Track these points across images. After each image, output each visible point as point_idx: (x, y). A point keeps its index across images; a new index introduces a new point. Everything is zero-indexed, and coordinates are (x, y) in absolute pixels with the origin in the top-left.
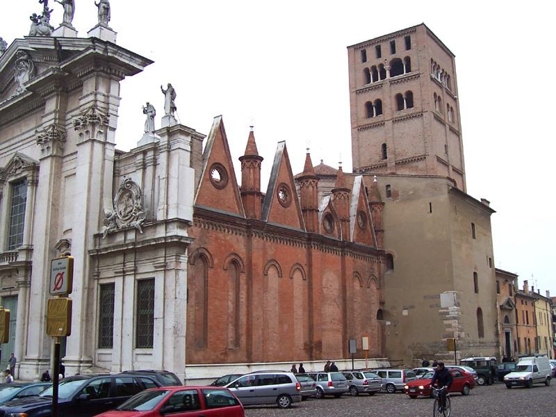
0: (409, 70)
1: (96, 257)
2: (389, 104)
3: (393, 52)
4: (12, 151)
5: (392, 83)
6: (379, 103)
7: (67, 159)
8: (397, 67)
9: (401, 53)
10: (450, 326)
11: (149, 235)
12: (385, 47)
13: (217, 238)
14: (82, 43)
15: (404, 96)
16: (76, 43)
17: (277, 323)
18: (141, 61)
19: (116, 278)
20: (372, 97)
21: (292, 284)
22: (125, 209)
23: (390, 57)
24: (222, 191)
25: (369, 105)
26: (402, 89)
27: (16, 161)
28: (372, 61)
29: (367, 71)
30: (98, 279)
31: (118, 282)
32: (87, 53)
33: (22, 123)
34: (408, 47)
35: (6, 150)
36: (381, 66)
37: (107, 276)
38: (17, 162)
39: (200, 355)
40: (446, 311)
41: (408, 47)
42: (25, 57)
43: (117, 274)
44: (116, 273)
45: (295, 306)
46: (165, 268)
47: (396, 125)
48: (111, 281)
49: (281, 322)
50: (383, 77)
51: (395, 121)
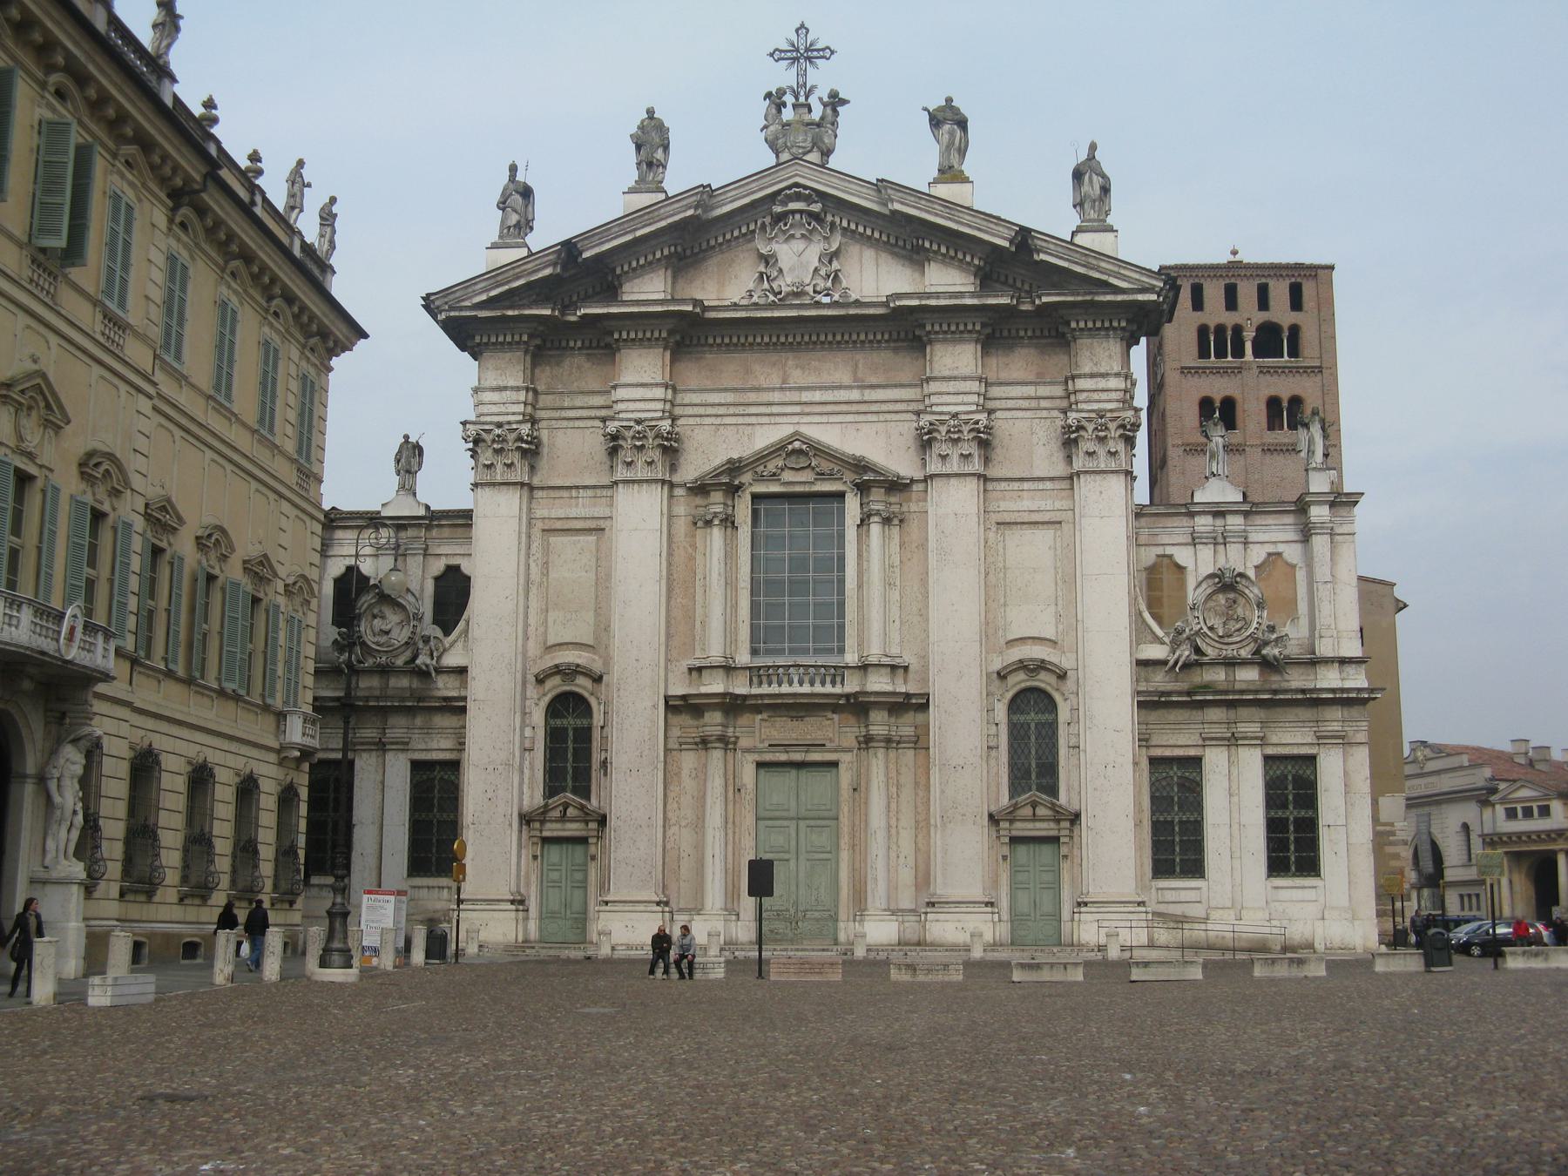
0: (1294, 352)
1: (1148, 704)
2: (1253, 414)
3: (1263, 304)
4: (765, 420)
5: (1264, 371)
6: (1229, 406)
7: (1003, 485)
8: (1270, 340)
9: (1281, 315)
10: (1396, 856)
11: (1296, 680)
12: (1247, 293)
14: (1122, 271)
15: (1285, 404)
16: (1103, 265)
19: (1208, 750)
20: (1218, 388)
22: (1224, 623)
23: (1260, 317)
25: (1206, 405)
26: (1285, 388)
27: (794, 451)
28: (1215, 313)
29: (1203, 331)
30: (1148, 747)
31: (1215, 761)
32: (1140, 297)
33: (790, 360)
34: (1296, 303)
35: (722, 410)
36: (1238, 330)
37: (1178, 739)
38: (799, 451)
40: (1388, 828)
41: (1296, 303)
42: (816, 207)
43: (1207, 741)
44: (1204, 739)
46: (1344, 741)
47: (1268, 458)
48: (1192, 752)
50: (1239, 352)
51: (1269, 450)
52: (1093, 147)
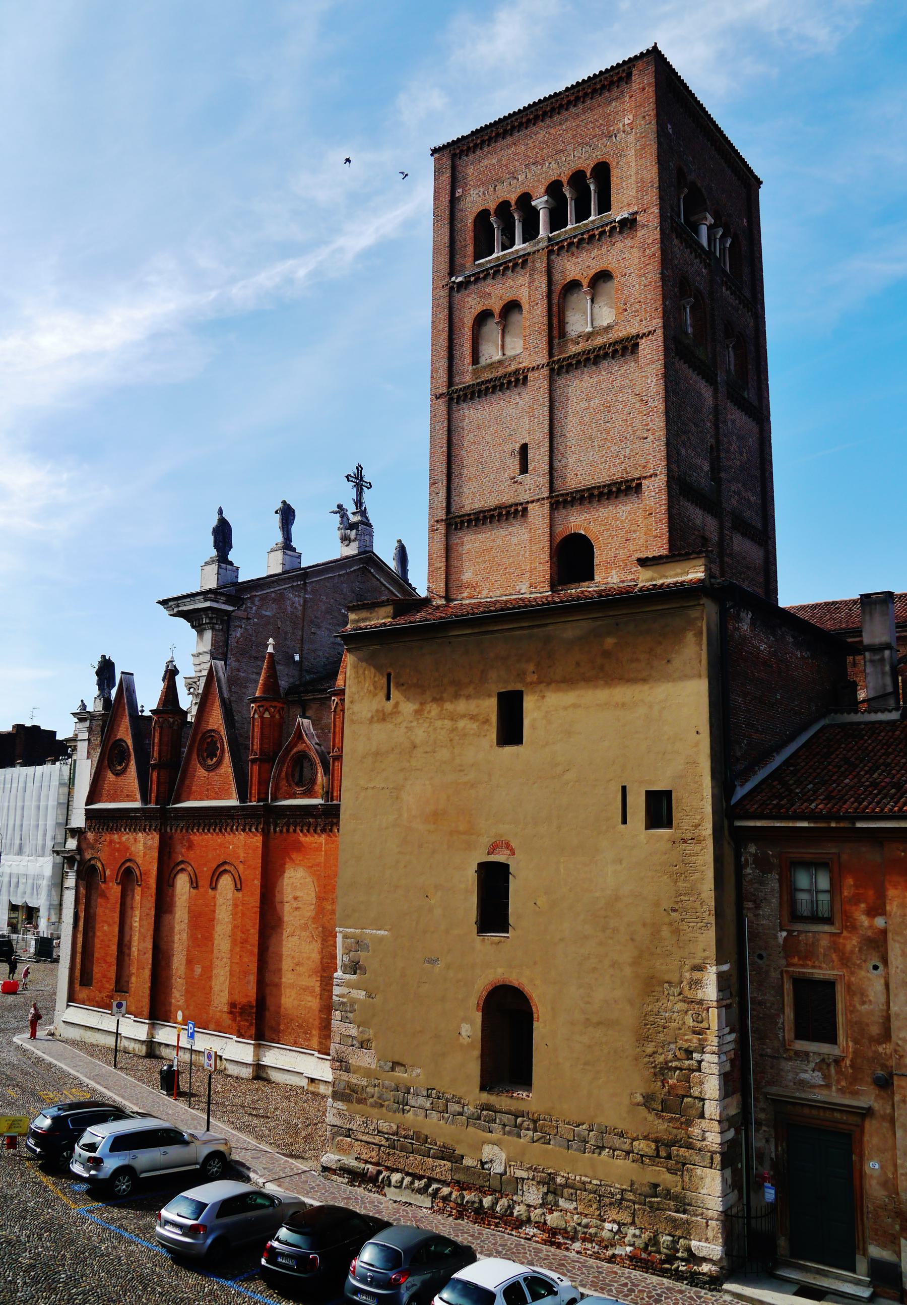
13: (111, 841)
17: (184, 962)
18: (202, 597)
21: (214, 898)
24: (122, 777)
39: (83, 994)
45: (216, 936)
49: (190, 962)
52: (220, 511)
